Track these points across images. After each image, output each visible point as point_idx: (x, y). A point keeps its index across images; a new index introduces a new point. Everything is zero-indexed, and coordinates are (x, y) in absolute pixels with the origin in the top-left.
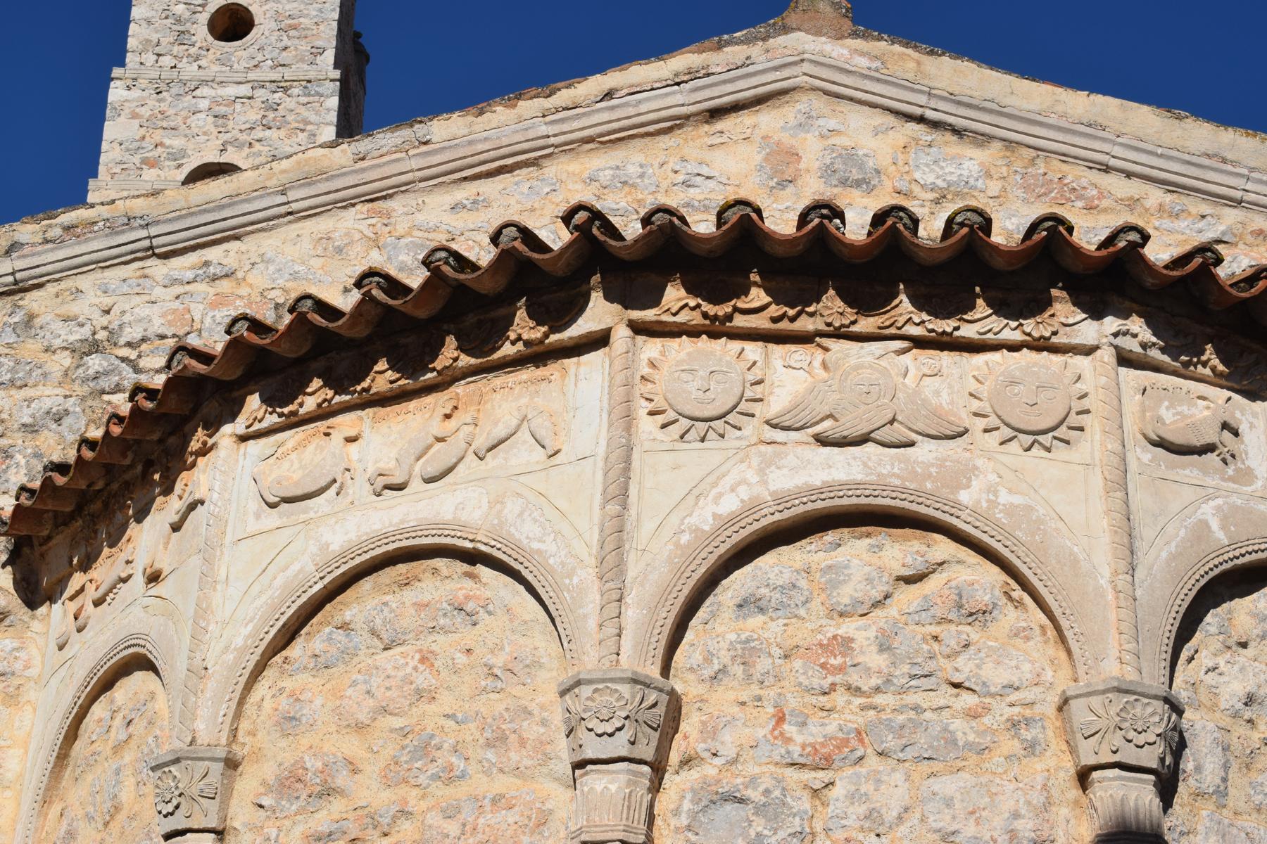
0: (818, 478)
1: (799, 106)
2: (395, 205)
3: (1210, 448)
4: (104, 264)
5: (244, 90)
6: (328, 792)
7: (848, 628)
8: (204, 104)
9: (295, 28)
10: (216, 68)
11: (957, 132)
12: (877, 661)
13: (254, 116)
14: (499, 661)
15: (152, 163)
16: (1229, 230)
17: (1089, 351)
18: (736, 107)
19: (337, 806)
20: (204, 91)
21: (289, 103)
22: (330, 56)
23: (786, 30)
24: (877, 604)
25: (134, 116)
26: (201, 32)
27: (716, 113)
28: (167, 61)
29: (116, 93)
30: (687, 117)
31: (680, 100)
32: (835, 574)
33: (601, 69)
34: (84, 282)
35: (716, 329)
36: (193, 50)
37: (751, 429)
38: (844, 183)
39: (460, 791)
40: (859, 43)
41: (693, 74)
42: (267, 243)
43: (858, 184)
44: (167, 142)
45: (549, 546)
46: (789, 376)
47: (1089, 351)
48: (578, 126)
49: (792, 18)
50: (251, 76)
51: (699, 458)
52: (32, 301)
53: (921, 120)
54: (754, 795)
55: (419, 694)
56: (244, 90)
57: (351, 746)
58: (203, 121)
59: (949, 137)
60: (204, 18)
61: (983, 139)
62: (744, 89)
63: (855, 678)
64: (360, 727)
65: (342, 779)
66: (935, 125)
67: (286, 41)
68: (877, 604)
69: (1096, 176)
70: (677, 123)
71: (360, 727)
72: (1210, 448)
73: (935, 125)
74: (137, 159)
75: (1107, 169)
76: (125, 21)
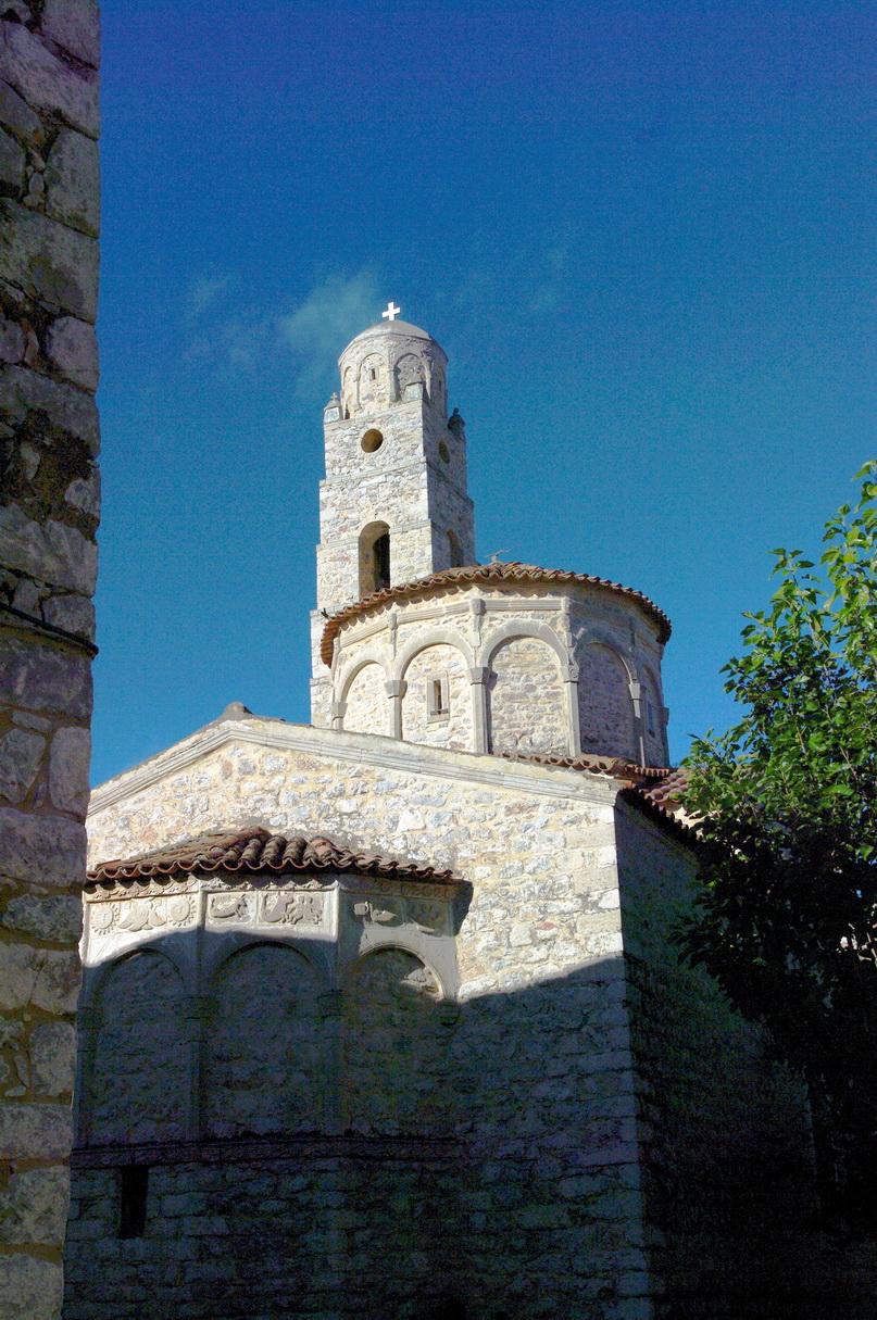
1: (232, 746)
2: (118, 805)
3: (233, 914)
5: (382, 478)
8: (364, 491)
9: (402, 436)
10: (368, 468)
11: (278, 748)
13: (388, 492)
15: (343, 529)
16: (358, 772)
17: (197, 892)
18: (213, 751)
20: (364, 483)
21: (404, 480)
22: (420, 450)
23: (224, 720)
24: (145, 976)
25: (333, 505)
26: (359, 450)
27: (207, 754)
28: (345, 470)
29: (323, 495)
30: (198, 757)
31: (195, 752)
33: (169, 747)
35: (107, 900)
36: (356, 461)
37: (116, 929)
38: (244, 773)
40: (246, 721)
41: (197, 742)
43: (249, 773)
44: (349, 516)
46: (126, 910)
47: (197, 892)
48: (168, 767)
49: (224, 715)
50: (384, 470)
51: (104, 939)
53: (266, 745)
54: (115, 1033)
56: (381, 478)
58: (364, 501)
59: (275, 750)
60: (359, 441)
61: (284, 750)
62: (214, 744)
63: (138, 998)
66: (271, 747)
67: (400, 445)
68: (145, 976)
69: (318, 758)
70: (195, 761)
72: (233, 914)
73: (271, 747)
74: (337, 529)
76: (322, 452)
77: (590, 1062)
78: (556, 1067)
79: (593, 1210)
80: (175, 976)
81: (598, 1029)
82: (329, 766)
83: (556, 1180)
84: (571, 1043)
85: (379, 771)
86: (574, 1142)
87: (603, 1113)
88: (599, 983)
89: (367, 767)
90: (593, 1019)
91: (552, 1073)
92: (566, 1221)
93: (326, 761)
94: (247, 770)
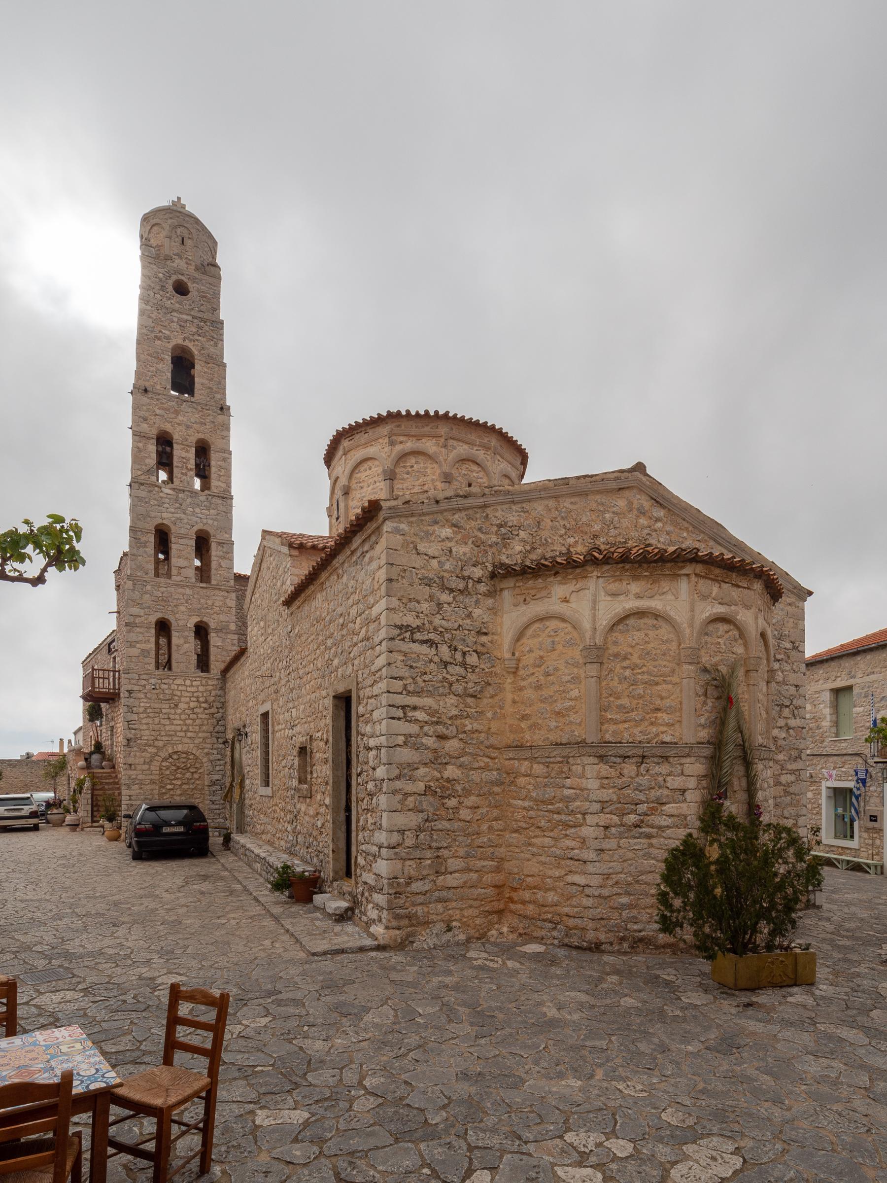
0: (719, 611)
4: (503, 503)
6: (625, 658)
7: (719, 640)
12: (724, 647)
14: (664, 638)
19: (628, 662)
32: (717, 629)
34: (499, 508)
39: (656, 663)
42: (535, 505)
45: (677, 617)
52: (488, 510)
55: (646, 642)
57: (630, 650)
64: (632, 647)
65: (629, 656)
71: (632, 647)
75: (684, 520)
77: (793, 723)
78: (781, 722)
79: (791, 790)
80: (740, 641)
81: (796, 708)
82: (687, 529)
83: (779, 775)
84: (786, 712)
85: (712, 543)
86: (786, 758)
87: (796, 746)
88: (797, 686)
89: (706, 538)
90: (794, 703)
91: (779, 725)
92: (782, 794)
93: (687, 525)
94: (642, 512)
